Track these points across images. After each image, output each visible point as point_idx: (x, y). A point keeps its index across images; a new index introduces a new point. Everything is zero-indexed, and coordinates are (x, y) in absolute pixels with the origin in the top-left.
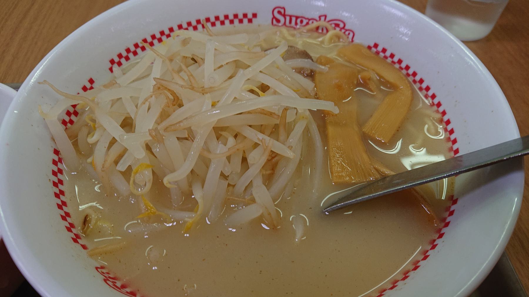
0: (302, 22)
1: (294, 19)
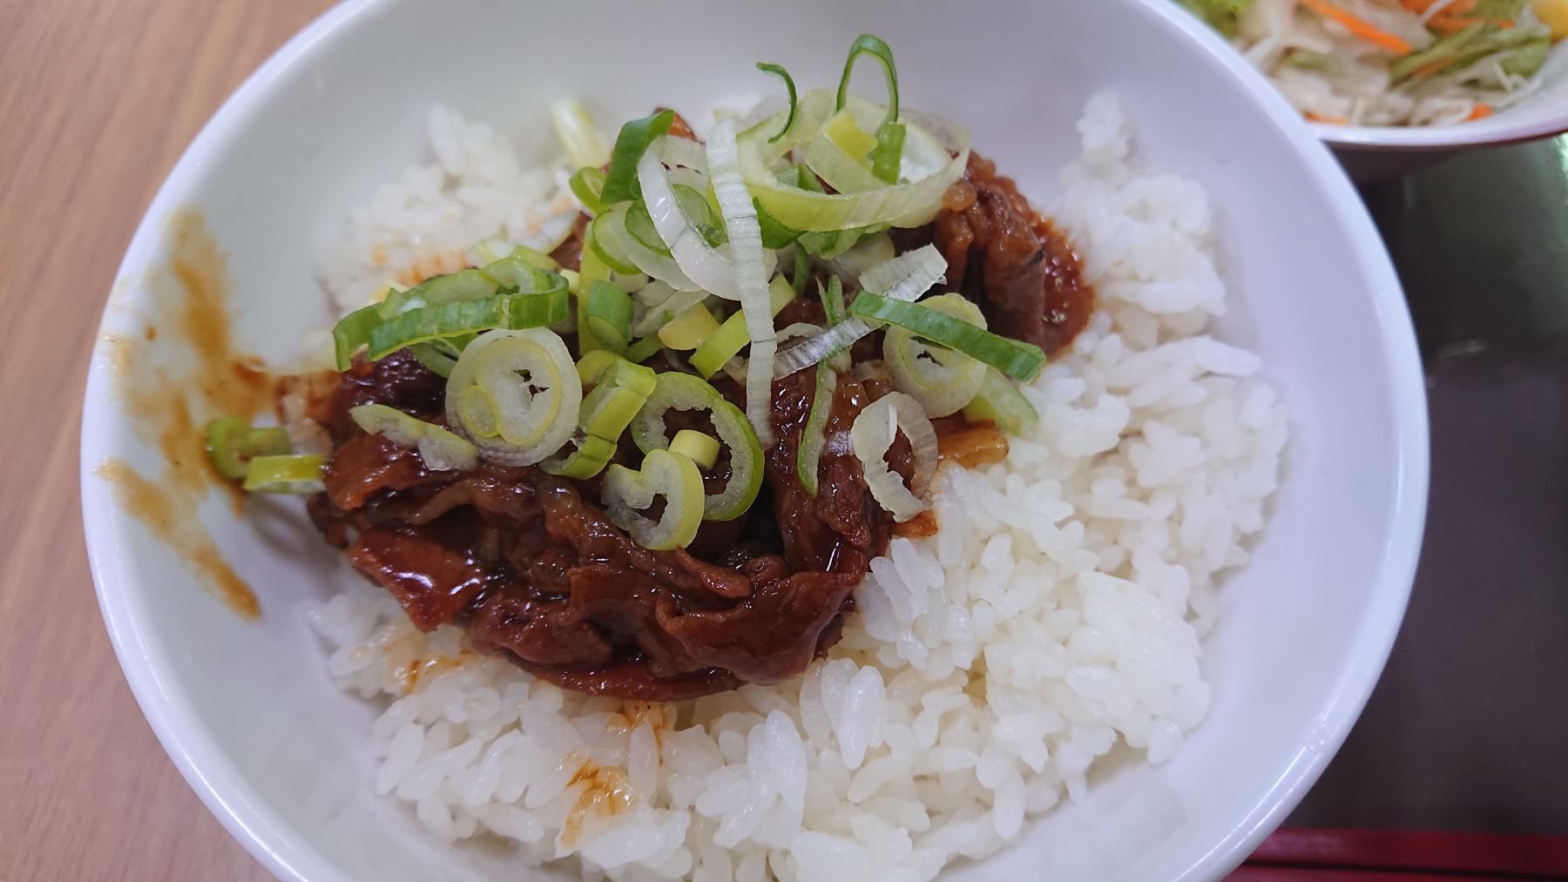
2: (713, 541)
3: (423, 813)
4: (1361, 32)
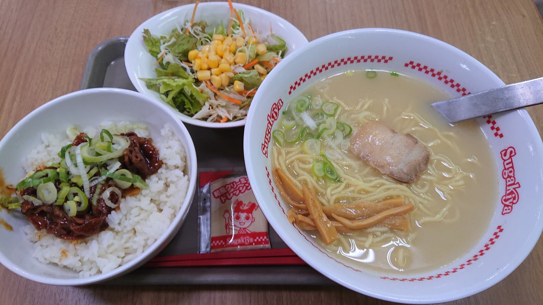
0: (511, 172)
1: (511, 165)
2: (80, 215)
3: (39, 259)
4: (230, 99)
